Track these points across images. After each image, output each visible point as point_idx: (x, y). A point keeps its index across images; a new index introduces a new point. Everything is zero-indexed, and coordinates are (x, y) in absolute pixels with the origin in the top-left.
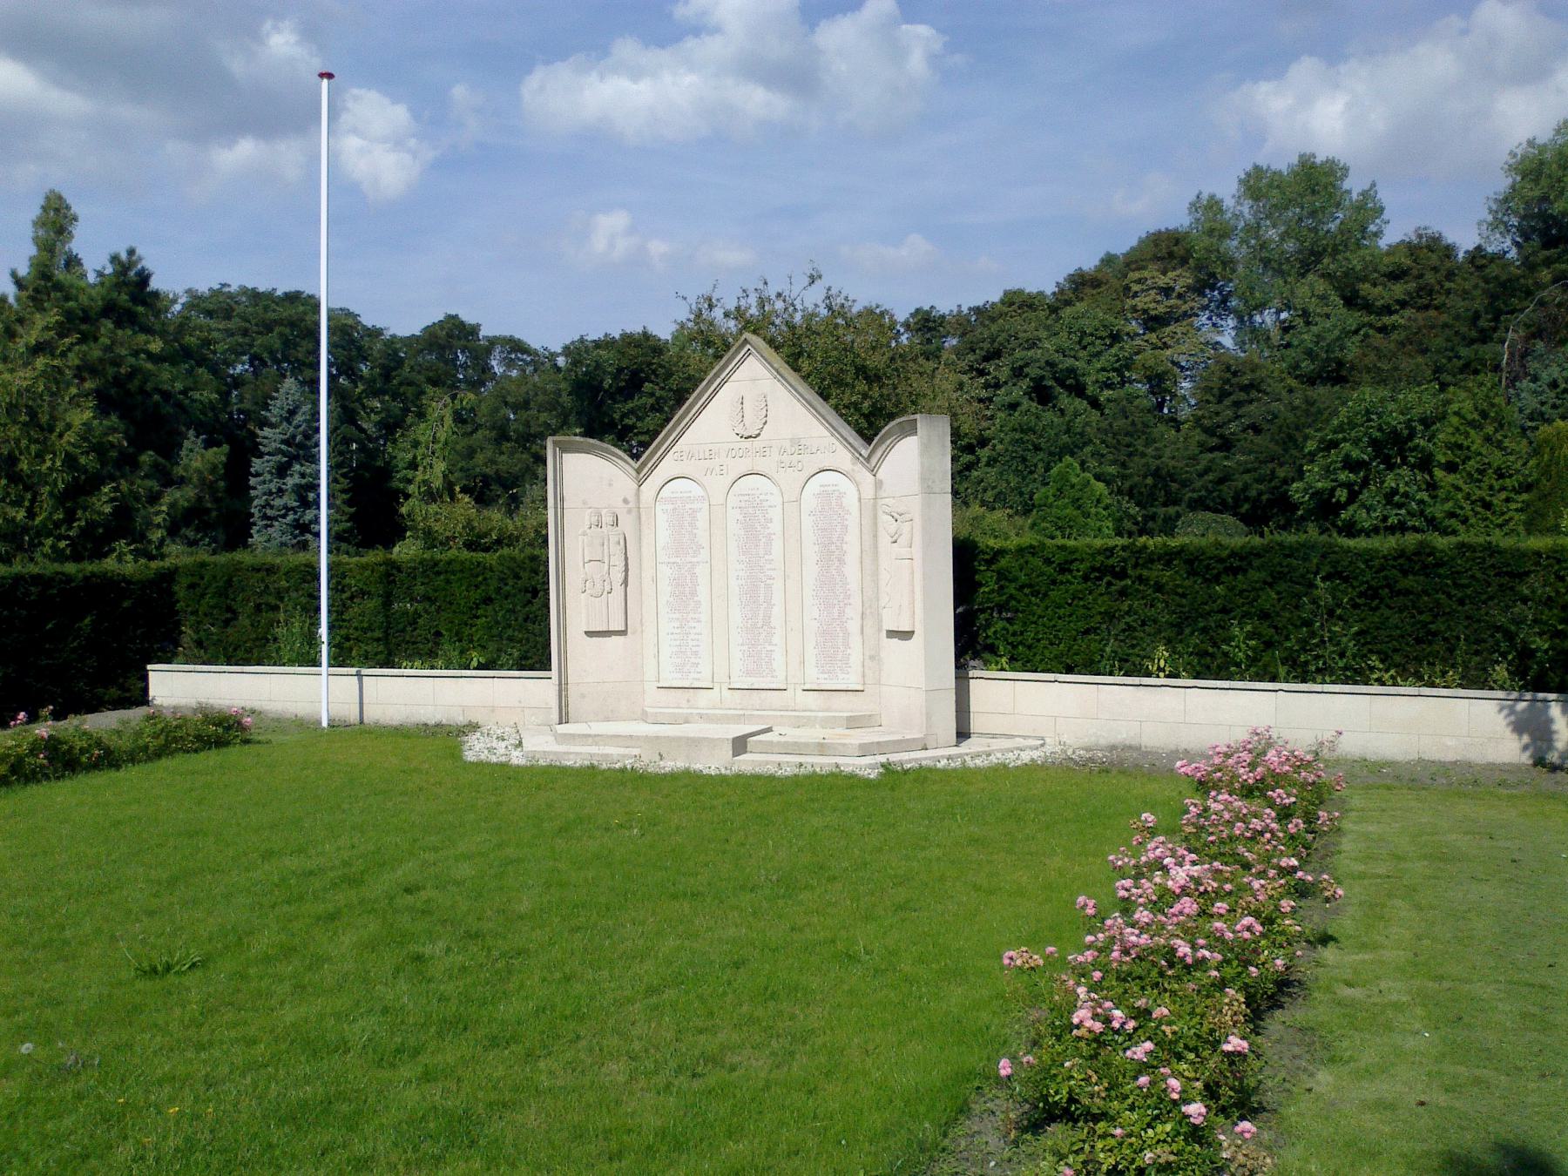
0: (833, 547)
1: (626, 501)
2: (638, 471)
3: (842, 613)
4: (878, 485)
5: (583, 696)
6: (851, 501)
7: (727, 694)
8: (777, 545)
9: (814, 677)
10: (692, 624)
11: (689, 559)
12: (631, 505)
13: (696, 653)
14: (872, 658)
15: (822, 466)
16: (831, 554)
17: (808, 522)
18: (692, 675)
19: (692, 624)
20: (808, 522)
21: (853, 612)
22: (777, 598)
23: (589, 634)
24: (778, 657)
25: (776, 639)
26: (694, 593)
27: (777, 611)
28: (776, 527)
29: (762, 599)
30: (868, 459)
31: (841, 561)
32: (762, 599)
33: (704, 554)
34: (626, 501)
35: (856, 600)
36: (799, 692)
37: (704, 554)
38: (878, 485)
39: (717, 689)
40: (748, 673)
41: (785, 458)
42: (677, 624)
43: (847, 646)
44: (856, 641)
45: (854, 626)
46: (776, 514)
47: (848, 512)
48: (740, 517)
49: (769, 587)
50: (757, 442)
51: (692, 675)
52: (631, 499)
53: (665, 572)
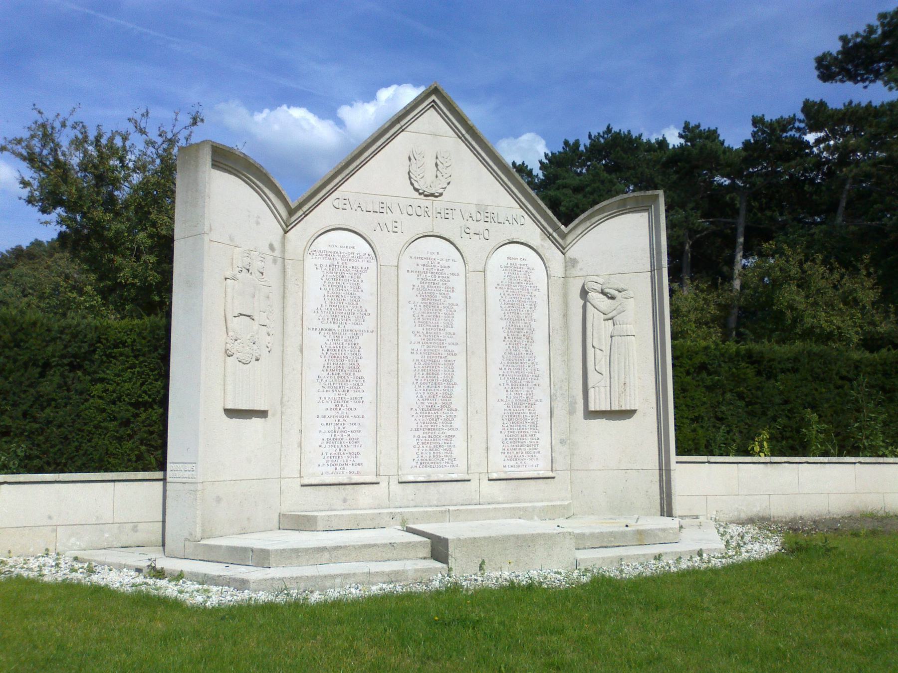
0: (521, 324)
1: (272, 247)
2: (291, 212)
3: (530, 394)
4: (571, 263)
5: (218, 500)
6: (539, 274)
7: (396, 488)
9: (500, 465)
10: (351, 405)
11: (349, 326)
12: (277, 253)
14: (562, 442)
16: (518, 334)
17: (494, 296)
18: (349, 468)
19: (351, 405)
21: (541, 395)
22: (459, 376)
23: (232, 413)
24: (459, 442)
25: (458, 423)
26: (355, 367)
27: (459, 391)
28: (458, 297)
30: (564, 236)
31: (530, 339)
32: (441, 377)
33: (370, 323)
34: (272, 247)
35: (544, 381)
36: (485, 481)
37: (370, 323)
38: (571, 263)
39: (384, 484)
40: (423, 463)
41: (470, 223)
43: (535, 428)
44: (544, 422)
45: (542, 409)
46: (458, 283)
47: (536, 289)
49: (450, 363)
50: (438, 203)
51: (349, 468)
52: (277, 245)
53: (316, 342)
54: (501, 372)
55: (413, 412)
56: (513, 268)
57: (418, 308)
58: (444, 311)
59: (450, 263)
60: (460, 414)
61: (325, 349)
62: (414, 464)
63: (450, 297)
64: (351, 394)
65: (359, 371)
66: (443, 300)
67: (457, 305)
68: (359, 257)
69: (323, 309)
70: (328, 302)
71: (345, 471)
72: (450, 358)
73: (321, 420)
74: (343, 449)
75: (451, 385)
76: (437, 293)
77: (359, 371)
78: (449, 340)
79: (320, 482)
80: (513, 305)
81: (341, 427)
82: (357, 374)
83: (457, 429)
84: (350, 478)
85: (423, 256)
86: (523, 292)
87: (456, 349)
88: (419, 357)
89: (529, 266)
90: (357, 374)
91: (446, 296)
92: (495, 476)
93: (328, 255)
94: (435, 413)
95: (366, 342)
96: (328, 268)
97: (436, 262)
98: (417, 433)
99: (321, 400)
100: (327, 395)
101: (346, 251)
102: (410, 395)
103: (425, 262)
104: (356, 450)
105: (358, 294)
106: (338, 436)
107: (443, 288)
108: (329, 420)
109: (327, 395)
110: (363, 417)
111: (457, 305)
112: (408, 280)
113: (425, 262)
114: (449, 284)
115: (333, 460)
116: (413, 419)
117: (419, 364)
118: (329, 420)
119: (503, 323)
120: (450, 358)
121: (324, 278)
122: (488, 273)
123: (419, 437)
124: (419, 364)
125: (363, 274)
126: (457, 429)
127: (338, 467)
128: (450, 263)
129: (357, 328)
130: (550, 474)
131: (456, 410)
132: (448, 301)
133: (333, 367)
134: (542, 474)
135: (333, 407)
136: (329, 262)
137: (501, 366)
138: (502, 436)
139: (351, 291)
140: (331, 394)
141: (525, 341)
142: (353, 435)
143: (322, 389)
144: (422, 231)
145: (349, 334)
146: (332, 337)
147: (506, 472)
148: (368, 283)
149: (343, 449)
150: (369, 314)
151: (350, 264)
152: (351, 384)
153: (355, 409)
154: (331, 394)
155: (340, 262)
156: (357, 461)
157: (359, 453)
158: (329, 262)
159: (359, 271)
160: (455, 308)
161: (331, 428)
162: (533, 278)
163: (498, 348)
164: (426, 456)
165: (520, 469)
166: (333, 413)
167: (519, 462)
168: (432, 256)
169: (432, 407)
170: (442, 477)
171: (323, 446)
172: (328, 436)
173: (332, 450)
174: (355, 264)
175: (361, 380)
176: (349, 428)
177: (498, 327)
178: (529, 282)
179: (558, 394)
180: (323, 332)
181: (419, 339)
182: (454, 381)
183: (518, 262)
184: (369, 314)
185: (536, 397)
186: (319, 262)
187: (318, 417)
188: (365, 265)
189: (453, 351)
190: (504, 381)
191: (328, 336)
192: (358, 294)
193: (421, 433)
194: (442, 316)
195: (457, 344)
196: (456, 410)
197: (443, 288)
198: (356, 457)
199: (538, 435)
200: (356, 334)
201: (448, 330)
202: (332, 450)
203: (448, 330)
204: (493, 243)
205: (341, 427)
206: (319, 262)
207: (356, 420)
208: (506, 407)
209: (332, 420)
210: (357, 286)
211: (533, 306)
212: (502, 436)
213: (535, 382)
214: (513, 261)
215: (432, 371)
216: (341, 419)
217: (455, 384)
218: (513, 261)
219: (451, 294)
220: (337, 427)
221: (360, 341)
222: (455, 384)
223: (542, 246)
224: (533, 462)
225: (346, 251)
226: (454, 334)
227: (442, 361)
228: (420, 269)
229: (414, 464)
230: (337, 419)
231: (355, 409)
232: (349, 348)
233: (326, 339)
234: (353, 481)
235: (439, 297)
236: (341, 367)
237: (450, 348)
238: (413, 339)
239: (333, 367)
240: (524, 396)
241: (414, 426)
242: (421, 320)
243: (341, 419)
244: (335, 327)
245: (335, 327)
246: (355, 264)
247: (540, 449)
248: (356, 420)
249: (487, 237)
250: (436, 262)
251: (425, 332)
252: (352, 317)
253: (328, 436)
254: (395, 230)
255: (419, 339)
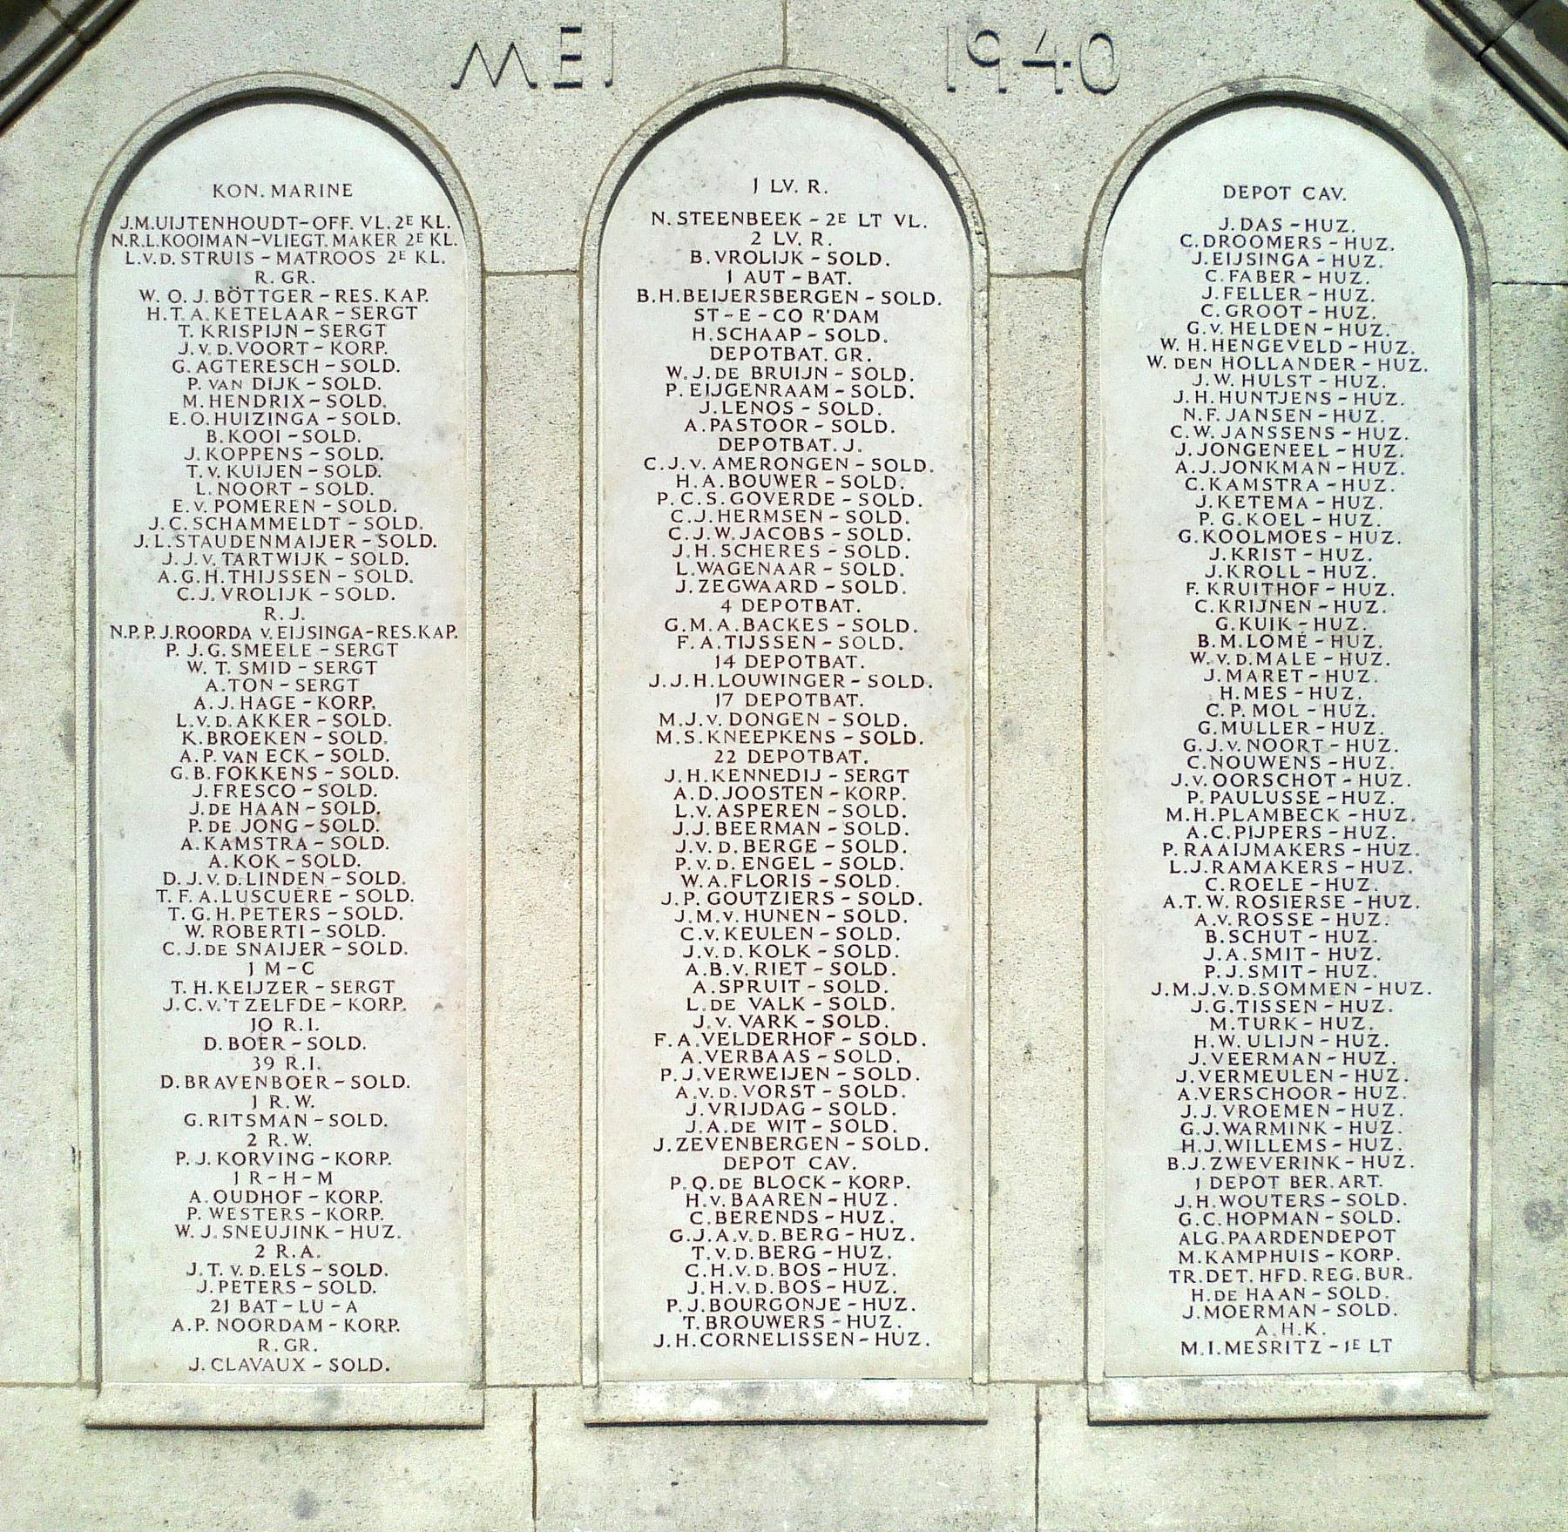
0: (1304, 561)
3: (1349, 950)
7: (571, 1454)
8: (936, 539)
10: (337, 1021)
11: (322, 609)
13: (363, 1206)
15: (1243, 72)
16: (1284, 609)
18: (331, 1343)
19: (337, 1021)
20: (1139, 409)
22: (931, 861)
26: (355, 823)
27: (926, 942)
28: (929, 423)
29: (824, 864)
31: (1354, 644)
32: (824, 864)
35: (1440, 881)
36: (1067, 1435)
37: (436, 583)
39: (507, 1429)
40: (724, 1321)
42: (240, 1024)
43: (1376, 1141)
44: (1433, 1112)
45: (1424, 1035)
47: (1403, 358)
48: (695, 357)
49: (881, 787)
51: (331, 1343)
54: (1177, 834)
55: (671, 1055)
56: (1258, 250)
57: (700, 495)
58: (847, 500)
59: (886, 238)
60: (933, 1063)
61: (200, 734)
62: (673, 1325)
63: (882, 427)
64: (334, 964)
65: (379, 843)
66: (840, 440)
67: (921, 466)
68: (382, 234)
69: (186, 521)
70: (210, 485)
71: (309, 1358)
72: (878, 757)
73: (185, 1099)
74: (294, 1246)
75: (879, 906)
76: (807, 408)
77: (379, 843)
78: (875, 661)
79: (174, 1416)
80: (1250, 456)
81: (285, 1135)
82: (368, 860)
83: (914, 1144)
84: (332, 1398)
85: (729, 204)
86: (1321, 380)
87: (909, 708)
88: (702, 757)
89: (1358, 228)
90: (368, 860)
91: (851, 421)
92: (1126, 1400)
93: (206, 239)
94: (793, 1060)
95: (418, 695)
96: (208, 309)
97: (804, 232)
98: (689, 1166)
99: (188, 996)
100: (212, 970)
101: (307, 208)
102: (653, 967)
103: (739, 237)
104: (365, 1252)
105: (367, 436)
106: (271, 1178)
107: (840, 380)
108: (221, 1100)
109: (212, 970)
110: (399, 1082)
111: (921, 466)
112: (646, 349)
113: (739, 237)
114: (877, 355)
115: (248, 1301)
116: (671, 1086)
117: (705, 793)
118: (221, 1100)
119: (1196, 561)
120: (878, 757)
121: (191, 363)
122: (1106, 278)
123: (700, 1182)
124: (705, 793)
125: (393, 327)
126: (914, 1144)
127: (275, 1338)
128: (886, 238)
129: (365, 615)
130: (1462, 1397)
131: (911, 1039)
132: (872, 447)
133: (237, 822)
134: (1410, 1391)
135: (243, 1030)
136: (212, 277)
137: (1178, 799)
138: (1181, 1183)
139: (331, 420)
140: (232, 968)
141: (1326, 658)
142: (346, 1178)
143: (182, 941)
144: (722, 63)
145: (325, 651)
146: (233, 666)
147: (1194, 1381)
148: (425, 374)
149: (294, 1246)
150: (427, 542)
151: (324, 279)
152: (332, 914)
153: (355, 1043)
154: (232, 968)
155: (273, 270)
156: (369, 1307)
157: (376, 1269)
158: (212, 277)
159: (373, 311)
160: (911, 482)
161: (235, 1139)
162: (1385, 293)
163: (1158, 702)
164: (740, 1283)
165: (1282, 1362)
166: (243, 1062)
167: (1273, 1324)
168: (774, 203)
169: (774, 1025)
170: (823, 1398)
171: (197, 1227)
172: (222, 1178)
173: (241, 1251)
174: (350, 277)
175: (389, 891)
176: (324, 1141)
177: (1161, 579)
178: (1358, 320)
179: (1522, 954)
180: (184, 646)
181: (700, 660)
182: (901, 881)
183: (1293, 210)
184: (427, 542)
185: (1381, 971)
186: (160, 278)
187: (167, 1081)
188: (405, 276)
189: (893, 719)
190: (1195, 885)
191: (209, 664)
192: (367, 436)
193: (710, 1163)
194: (835, 525)
195: (918, 682)
196: (911, 1039)
197: (840, 380)
198: (367, 1289)
199: (1390, 1180)
200: (358, 648)
201: (868, 605)
202: (241, 1251)
203: (868, 605)
204: (1139, 111)
205: (285, 1135)
206: (160, 278)
207: (364, 1101)
208: (1204, 1027)
209: (239, 1100)
210: (360, 398)
211: (1382, 454)
212: (1181, 1183)
213: (1381, 884)
214: (1259, 208)
215: (786, 840)
216: (286, 1096)
217: (909, 898)
218: (1259, 208)
219: (884, 408)
220: (263, 1133)
221: (382, 683)
222: (909, 898)
223: (1440, 109)
224: (1363, 1328)
225: (307, 208)
226: (903, 625)
227: (834, 777)
228: (711, 276)
229: (673, 1325)
230: (264, 1094)
231: (355, 1043)
232: (322, 723)
233: (201, 680)
234: (341, 1416)
235: (818, 425)
236: (281, 826)
237: (879, 703)
238: (671, 659)
239: (237, 822)
240: (1314, 966)
241: (676, 1125)
242: (715, 554)
243: (286, 1096)
244: (248, 614)
245: (248, 614)
246: (350, 277)
247: (1403, 1254)
248: (364, 1101)
249: (1101, 78)
250: (804, 232)
251: (735, 619)
252: (338, 563)
253: (222, 1178)
254: (571, 72)
255: (703, 661)
